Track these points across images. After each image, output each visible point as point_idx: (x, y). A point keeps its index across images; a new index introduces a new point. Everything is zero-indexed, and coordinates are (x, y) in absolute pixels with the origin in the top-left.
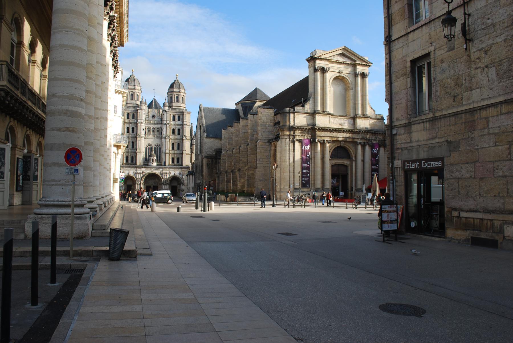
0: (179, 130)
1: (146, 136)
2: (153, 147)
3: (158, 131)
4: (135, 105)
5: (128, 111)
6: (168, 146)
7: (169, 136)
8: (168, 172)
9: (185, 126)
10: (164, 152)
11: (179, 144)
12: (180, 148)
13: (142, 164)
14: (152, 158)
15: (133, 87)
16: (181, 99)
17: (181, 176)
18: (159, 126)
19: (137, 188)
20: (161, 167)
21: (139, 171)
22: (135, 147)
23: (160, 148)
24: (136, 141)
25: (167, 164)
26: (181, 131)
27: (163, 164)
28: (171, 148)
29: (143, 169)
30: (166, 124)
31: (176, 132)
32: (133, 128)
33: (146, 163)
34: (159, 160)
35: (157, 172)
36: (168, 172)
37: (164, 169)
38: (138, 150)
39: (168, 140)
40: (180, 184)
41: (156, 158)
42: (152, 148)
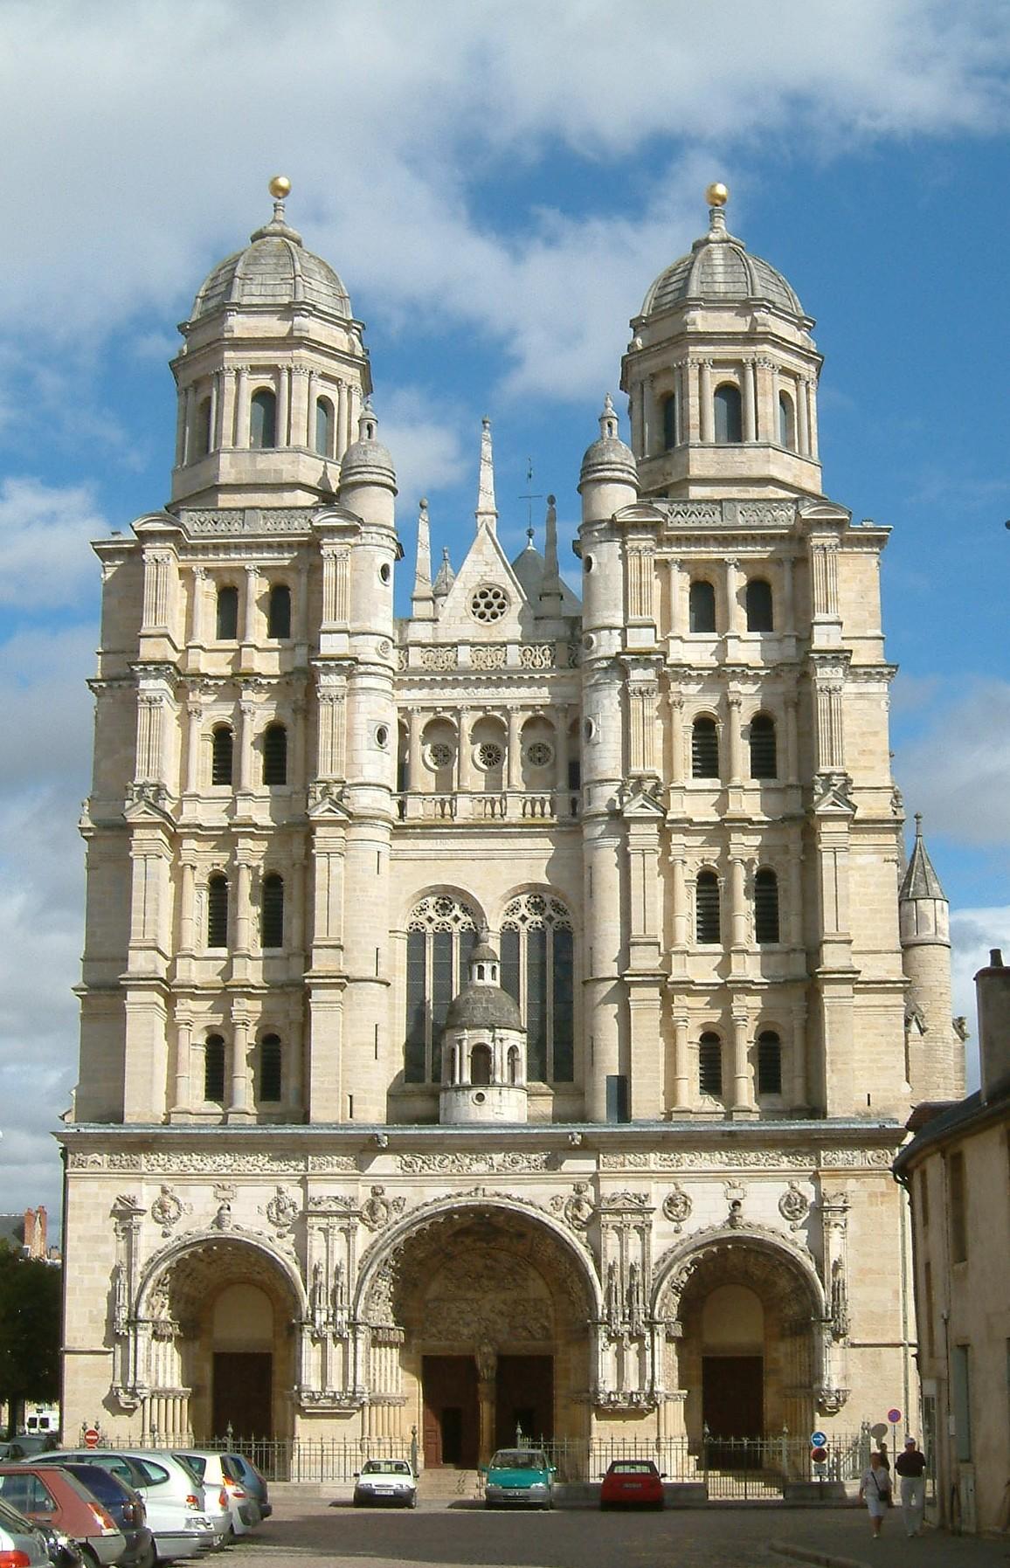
1: (418, 809)
2: (495, 922)
3: (536, 755)
5: (220, 560)
6: (645, 906)
7: (659, 794)
8: (658, 1193)
9: (825, 675)
12: (789, 924)
14: (470, 1038)
15: (274, 326)
16: (769, 409)
19: (311, 1379)
20: (576, 1131)
21: (333, 1183)
23: (565, 938)
25: (647, 1103)
30: (619, 666)
33: (420, 1106)
34: (559, 1056)
35: (537, 1193)
36: (658, 1193)
37: (610, 1161)
38: (322, 962)
39: (644, 836)
41: (517, 1039)
42: (473, 938)
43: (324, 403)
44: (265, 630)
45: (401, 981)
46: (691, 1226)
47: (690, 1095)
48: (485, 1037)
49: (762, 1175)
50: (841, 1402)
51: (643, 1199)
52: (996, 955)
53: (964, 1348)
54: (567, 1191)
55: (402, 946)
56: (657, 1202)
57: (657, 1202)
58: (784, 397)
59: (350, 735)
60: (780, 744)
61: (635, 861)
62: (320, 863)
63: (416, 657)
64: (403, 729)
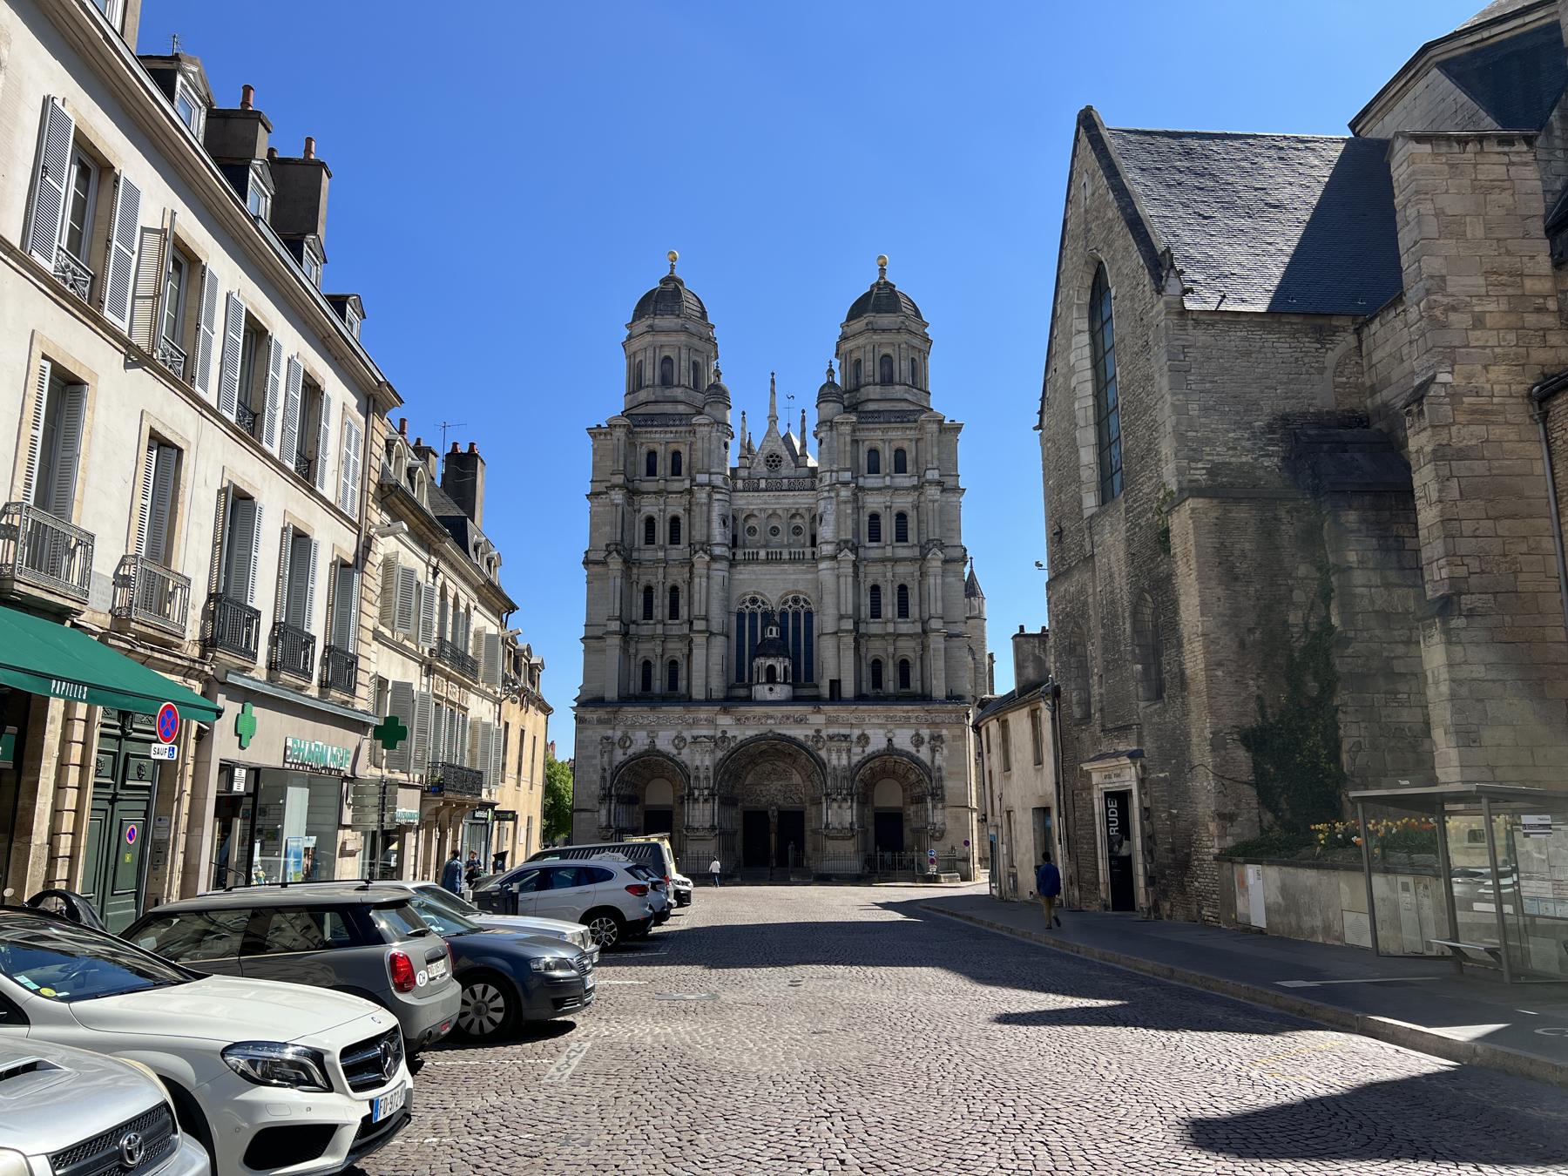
0: (901, 517)
1: (740, 555)
4: (681, 408)
10: (830, 627)
11: (903, 589)
12: (914, 610)
13: (718, 693)
17: (924, 754)
18: (802, 500)
22: (683, 611)
23: (809, 615)
24: (690, 582)
26: (912, 524)
27: (825, 691)
28: (866, 610)
29: (725, 721)
31: (888, 527)
32: (675, 521)
33: (742, 692)
35: (799, 733)
38: (699, 625)
40: (920, 800)
43: (695, 364)
44: (669, 471)
45: (734, 635)
46: (869, 749)
47: (867, 688)
48: (770, 662)
49: (901, 726)
50: (942, 835)
51: (846, 737)
52: (1022, 628)
53: (1009, 812)
54: (811, 733)
55: (734, 618)
56: (854, 738)
57: (854, 738)
58: (913, 360)
59: (709, 522)
60: (910, 526)
61: (842, 580)
62: (697, 580)
63: (740, 484)
64: (734, 518)
